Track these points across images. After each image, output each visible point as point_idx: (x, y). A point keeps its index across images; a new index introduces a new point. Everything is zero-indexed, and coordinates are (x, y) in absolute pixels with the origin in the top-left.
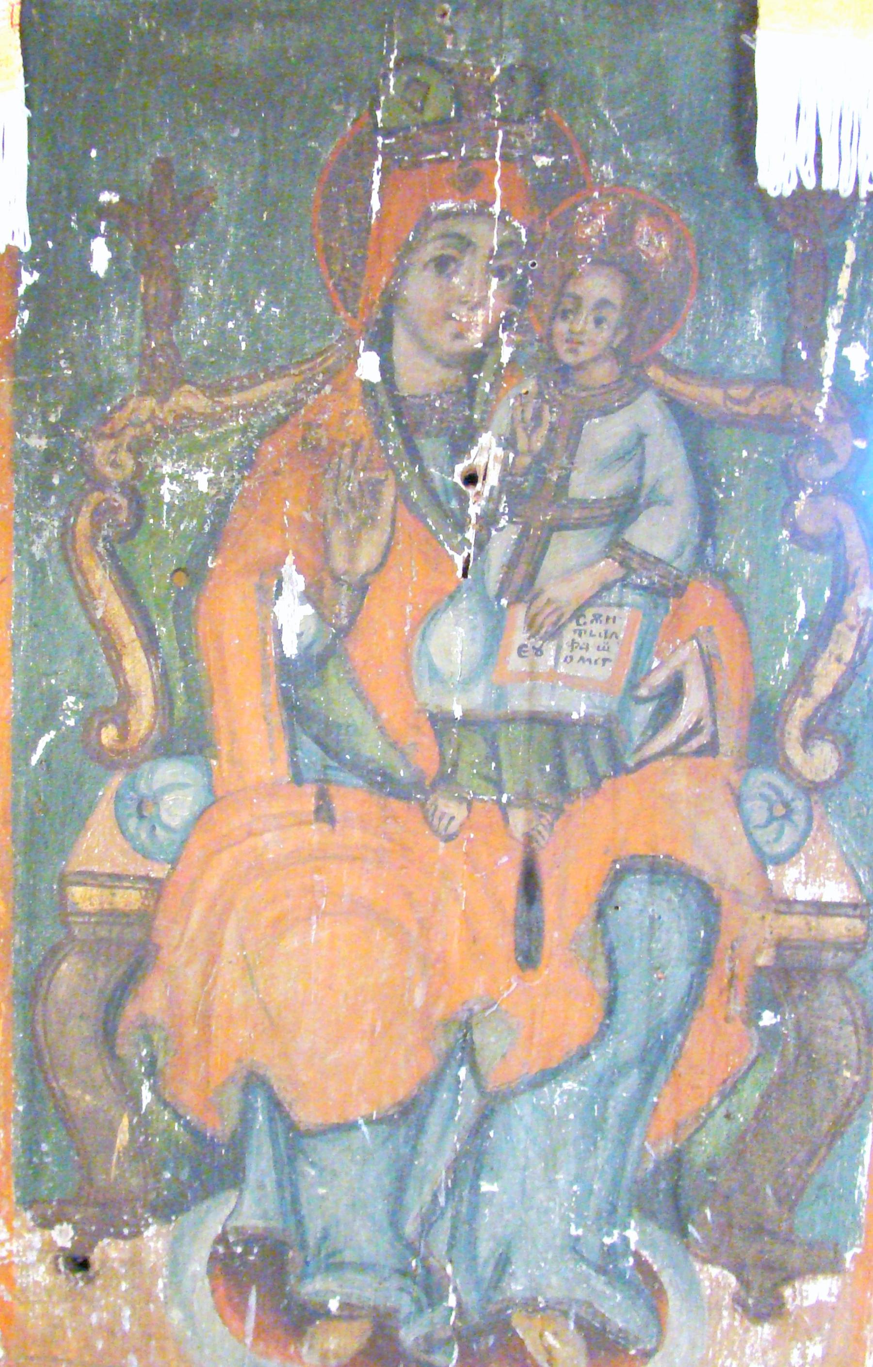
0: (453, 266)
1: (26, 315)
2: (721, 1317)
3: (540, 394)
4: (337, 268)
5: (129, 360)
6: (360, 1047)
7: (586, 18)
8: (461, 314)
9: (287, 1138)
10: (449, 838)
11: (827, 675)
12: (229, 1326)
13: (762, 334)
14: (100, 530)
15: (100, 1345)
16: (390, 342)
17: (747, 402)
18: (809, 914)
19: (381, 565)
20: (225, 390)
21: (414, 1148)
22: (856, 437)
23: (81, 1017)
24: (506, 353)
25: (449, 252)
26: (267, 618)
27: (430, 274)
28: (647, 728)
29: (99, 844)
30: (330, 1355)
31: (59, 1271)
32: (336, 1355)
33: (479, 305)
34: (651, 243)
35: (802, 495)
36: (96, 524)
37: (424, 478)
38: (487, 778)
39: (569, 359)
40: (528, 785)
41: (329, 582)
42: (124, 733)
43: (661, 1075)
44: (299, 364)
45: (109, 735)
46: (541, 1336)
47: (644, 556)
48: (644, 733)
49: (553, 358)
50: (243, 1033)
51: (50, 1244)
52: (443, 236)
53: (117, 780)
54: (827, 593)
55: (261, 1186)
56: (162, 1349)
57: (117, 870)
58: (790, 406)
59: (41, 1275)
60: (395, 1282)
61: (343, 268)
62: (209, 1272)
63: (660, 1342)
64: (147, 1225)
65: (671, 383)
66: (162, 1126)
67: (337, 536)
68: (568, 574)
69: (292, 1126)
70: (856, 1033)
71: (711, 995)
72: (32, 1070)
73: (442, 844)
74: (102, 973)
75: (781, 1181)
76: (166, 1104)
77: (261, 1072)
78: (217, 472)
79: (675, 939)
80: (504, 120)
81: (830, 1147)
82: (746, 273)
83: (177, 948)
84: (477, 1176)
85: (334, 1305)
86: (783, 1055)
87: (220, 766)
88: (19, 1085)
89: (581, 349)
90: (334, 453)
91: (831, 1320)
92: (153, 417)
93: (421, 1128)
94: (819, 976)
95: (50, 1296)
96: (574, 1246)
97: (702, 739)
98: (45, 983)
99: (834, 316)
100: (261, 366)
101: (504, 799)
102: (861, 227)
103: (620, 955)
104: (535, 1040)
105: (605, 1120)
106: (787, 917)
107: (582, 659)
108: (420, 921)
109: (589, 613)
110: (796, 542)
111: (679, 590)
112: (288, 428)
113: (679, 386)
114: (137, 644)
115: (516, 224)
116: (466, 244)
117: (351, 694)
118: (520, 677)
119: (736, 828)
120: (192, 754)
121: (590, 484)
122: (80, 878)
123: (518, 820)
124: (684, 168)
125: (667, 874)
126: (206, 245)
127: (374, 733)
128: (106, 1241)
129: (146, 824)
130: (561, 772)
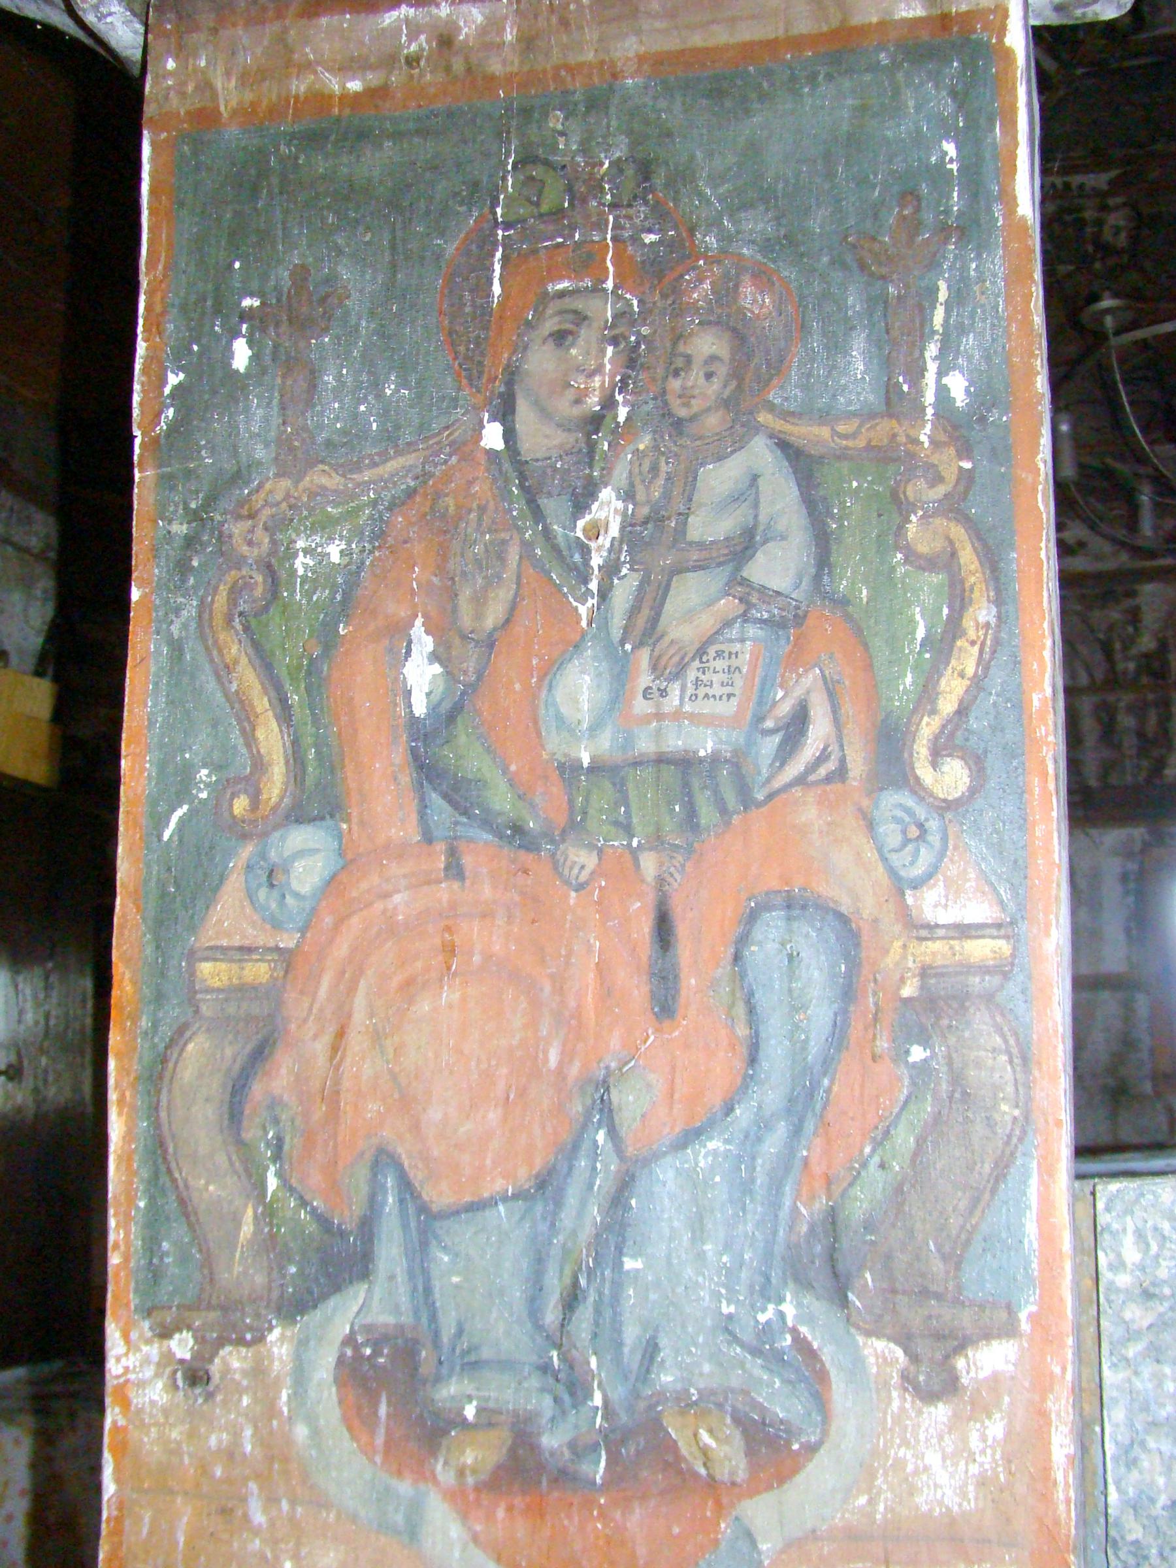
0: (570, 338)
1: (171, 412)
2: (890, 1398)
3: (656, 448)
4: (462, 349)
5: (267, 445)
6: (493, 1116)
7: (686, 111)
8: (579, 382)
9: (419, 1221)
10: (580, 887)
11: (951, 691)
12: (358, 1441)
13: (865, 372)
14: (235, 605)
15: (219, 1472)
16: (513, 412)
17: (854, 436)
18: (952, 938)
19: (507, 621)
20: (357, 467)
21: (553, 1224)
22: (961, 459)
23: (207, 1100)
24: (622, 413)
25: (568, 326)
26: (396, 679)
27: (550, 345)
28: (773, 762)
29: (230, 915)
30: (468, 1472)
31: (177, 1387)
32: (474, 1471)
33: (596, 369)
34: (755, 301)
35: (913, 518)
36: (233, 601)
37: (547, 534)
38: (616, 824)
39: (682, 413)
40: (658, 829)
41: (457, 641)
42: (255, 803)
43: (810, 1126)
44: (426, 439)
45: (240, 805)
46: (695, 1435)
47: (763, 590)
48: (771, 765)
49: (666, 413)
50: (373, 1108)
51: (168, 1357)
52: (561, 312)
53: (247, 851)
54: (945, 611)
55: (392, 1278)
56: (286, 1473)
57: (247, 943)
58: (894, 436)
59: (156, 1393)
60: (534, 1382)
61: (468, 349)
62: (336, 1380)
63: (825, 1433)
64: (271, 1328)
65: (778, 425)
66: (289, 1214)
67: (466, 593)
68: (689, 616)
69: (423, 1209)
70: (1011, 1062)
71: (856, 1031)
72: (155, 1162)
73: (573, 894)
74: (229, 1052)
75: (944, 1234)
76: (292, 1190)
77: (390, 1148)
78: (349, 544)
79: (817, 974)
80: (614, 206)
81: (994, 1191)
82: (847, 319)
83: (305, 1020)
84: (620, 1252)
85: (470, 1412)
86: (935, 1093)
87: (350, 829)
88: (142, 1181)
89: (693, 402)
90: (461, 519)
91: (1010, 1393)
92: (288, 496)
93: (559, 1202)
94: (967, 1004)
95: (167, 1417)
96: (727, 1325)
97: (831, 765)
98: (171, 1065)
99: (932, 350)
100: (390, 438)
101: (635, 843)
102: (951, 268)
103: (762, 999)
104: (677, 1096)
105: (753, 1180)
106: (929, 943)
107: (706, 696)
108: (552, 977)
109: (712, 651)
110: (911, 563)
111: (799, 619)
112: (418, 499)
113: (788, 427)
114: (270, 713)
115: (628, 296)
116: (581, 318)
117: (481, 750)
118: (646, 719)
119: (871, 855)
120: (323, 818)
121: (708, 526)
122: (206, 953)
123: (649, 864)
124: (782, 233)
125: (804, 907)
126: (339, 339)
127: (502, 785)
128: (228, 1348)
129: (275, 893)
130: (691, 813)
